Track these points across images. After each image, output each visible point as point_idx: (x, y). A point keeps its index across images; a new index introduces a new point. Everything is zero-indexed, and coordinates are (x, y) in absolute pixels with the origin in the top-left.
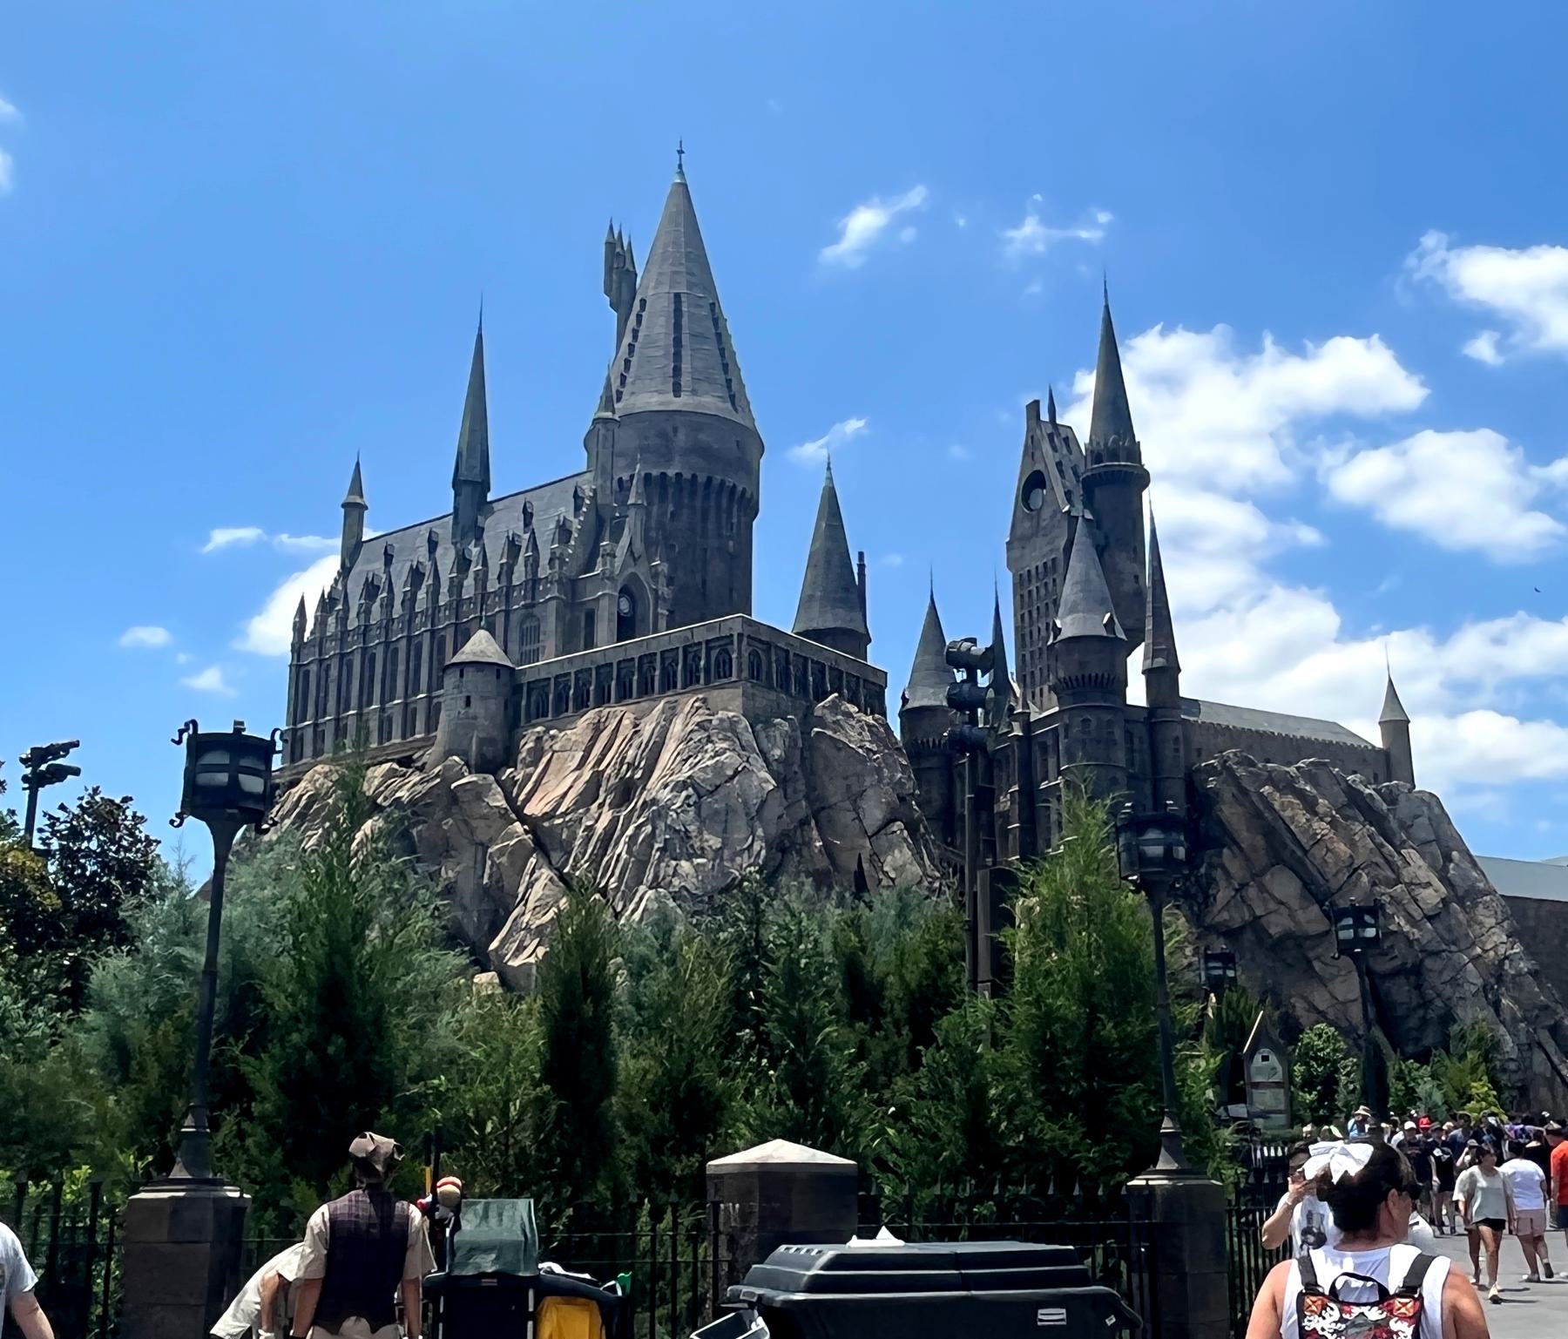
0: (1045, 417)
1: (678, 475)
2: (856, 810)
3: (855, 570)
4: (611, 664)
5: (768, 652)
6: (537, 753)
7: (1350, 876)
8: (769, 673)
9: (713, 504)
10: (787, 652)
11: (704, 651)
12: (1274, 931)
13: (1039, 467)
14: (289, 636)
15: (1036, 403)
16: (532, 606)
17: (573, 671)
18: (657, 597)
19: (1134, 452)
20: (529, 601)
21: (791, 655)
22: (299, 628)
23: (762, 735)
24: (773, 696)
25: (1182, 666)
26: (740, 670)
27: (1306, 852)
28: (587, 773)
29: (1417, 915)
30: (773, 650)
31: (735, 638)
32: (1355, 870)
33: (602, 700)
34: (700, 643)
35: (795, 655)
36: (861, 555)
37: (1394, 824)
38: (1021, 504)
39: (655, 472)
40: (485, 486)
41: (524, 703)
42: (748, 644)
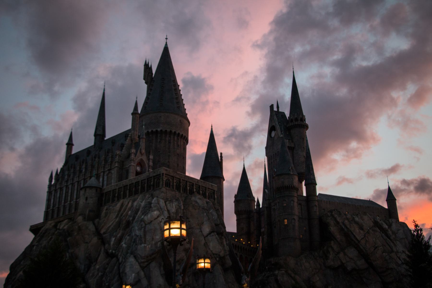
0: (275, 109)
1: (161, 130)
2: (200, 229)
3: (220, 158)
5: (173, 180)
6: (106, 214)
7: (375, 249)
8: (173, 186)
9: (172, 138)
10: (180, 179)
11: (153, 179)
12: (349, 268)
13: (274, 124)
14: (47, 183)
17: (117, 188)
18: (149, 166)
19: (303, 119)
20: (109, 168)
21: (181, 180)
22: (51, 180)
23: (168, 205)
24: (173, 193)
25: (317, 183)
26: (162, 185)
27: (359, 242)
28: (118, 219)
29: (400, 262)
30: (175, 179)
31: (161, 175)
32: (376, 247)
33: (125, 197)
34: (152, 177)
35: (182, 180)
36: (221, 154)
37: (390, 232)
39: (154, 130)
40: (104, 135)
41: (104, 199)
42: (166, 177)
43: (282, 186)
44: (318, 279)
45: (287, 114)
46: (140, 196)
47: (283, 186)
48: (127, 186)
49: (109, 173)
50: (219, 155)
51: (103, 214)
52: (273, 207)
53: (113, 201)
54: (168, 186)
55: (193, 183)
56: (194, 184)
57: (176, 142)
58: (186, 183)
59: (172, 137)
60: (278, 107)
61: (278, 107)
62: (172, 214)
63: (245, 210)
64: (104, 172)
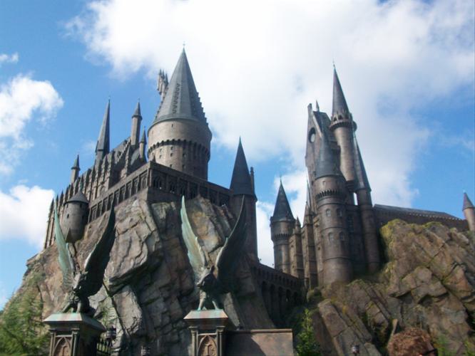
13: (313, 126)
15: (311, 104)
17: (102, 199)
35: (181, 179)
38: (309, 143)
44: (378, 311)
45: (330, 115)
46: (123, 203)
48: (112, 194)
49: (103, 187)
50: (250, 170)
51: (86, 234)
52: (315, 224)
53: (98, 215)
58: (186, 185)
59: (187, 147)
60: (318, 107)
61: (318, 107)
62: (160, 222)
64: (97, 187)
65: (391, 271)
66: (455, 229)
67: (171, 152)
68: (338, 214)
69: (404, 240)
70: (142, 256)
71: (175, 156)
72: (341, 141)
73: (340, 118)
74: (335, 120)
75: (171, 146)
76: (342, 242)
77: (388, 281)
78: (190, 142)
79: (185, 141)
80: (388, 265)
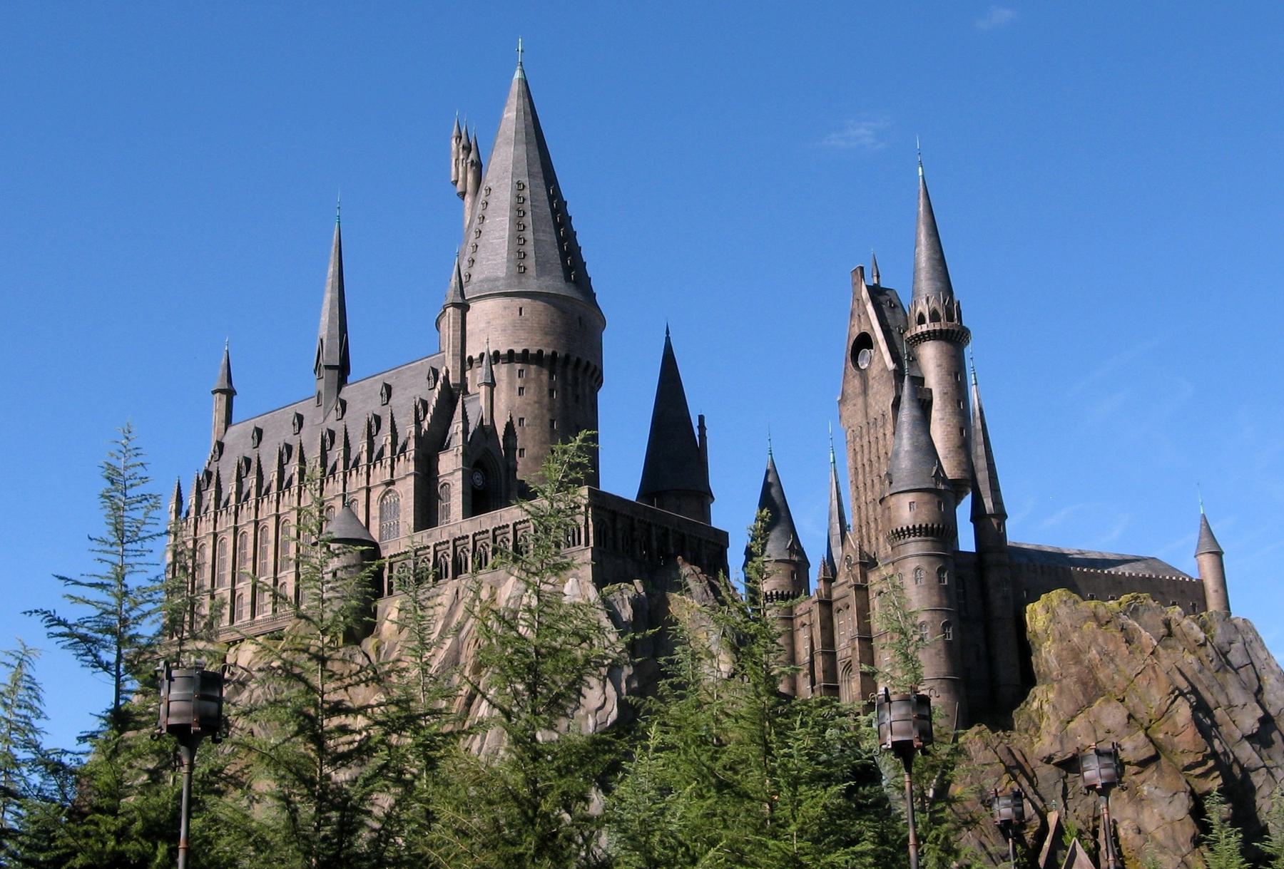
3: (697, 432)
4: (467, 537)
5: (614, 521)
10: (632, 519)
13: (865, 328)
15: (862, 268)
16: (392, 483)
17: (431, 544)
20: (388, 478)
21: (636, 521)
36: (701, 418)
43: (911, 527)
47: (914, 526)
49: (387, 493)
50: (695, 423)
54: (603, 543)
55: (667, 529)
56: (670, 532)
57: (569, 388)
63: (780, 592)
65: (1046, 707)
66: (1178, 609)
67: (519, 383)
68: (940, 580)
69: (1075, 638)
70: (608, 707)
71: (530, 395)
72: (934, 378)
73: (935, 317)
74: (921, 320)
75: (518, 366)
76: (949, 645)
77: (1038, 729)
78: (567, 357)
79: (554, 353)
80: (1038, 691)
